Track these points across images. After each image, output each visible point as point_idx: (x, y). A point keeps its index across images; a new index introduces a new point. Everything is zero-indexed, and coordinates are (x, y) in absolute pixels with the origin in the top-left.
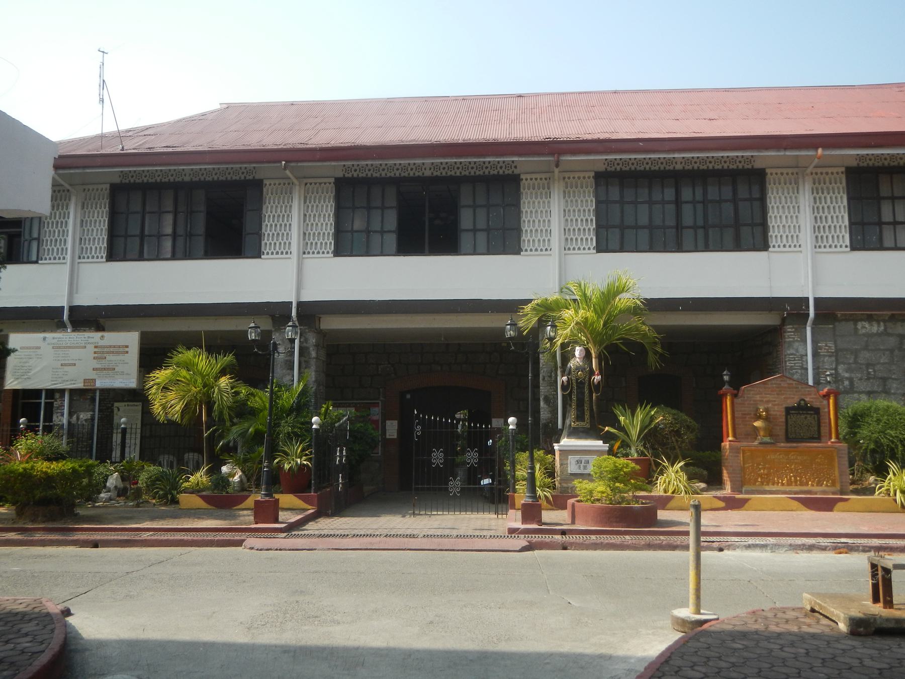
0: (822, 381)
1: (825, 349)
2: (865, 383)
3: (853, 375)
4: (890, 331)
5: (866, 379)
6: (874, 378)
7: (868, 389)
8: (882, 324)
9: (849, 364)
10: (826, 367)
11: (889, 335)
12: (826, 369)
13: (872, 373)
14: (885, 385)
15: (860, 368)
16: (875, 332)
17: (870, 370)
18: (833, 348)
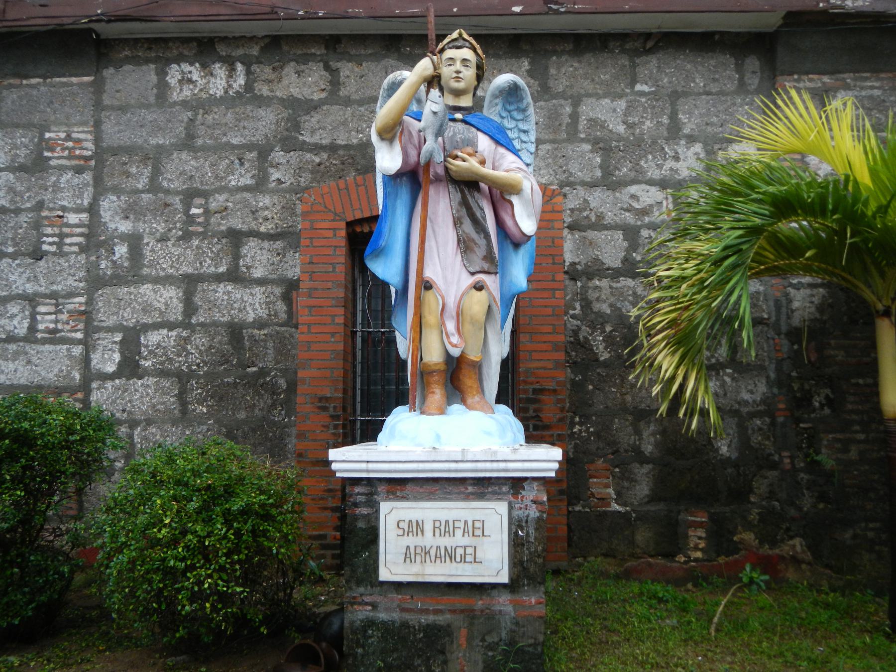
0: (45, 247)
1: (63, 149)
2: (176, 251)
3: (141, 227)
4: (264, 90)
5: (180, 239)
6: (203, 235)
7: (186, 269)
8: (239, 67)
9: (137, 192)
10: (65, 203)
11: (261, 101)
12: (64, 209)
13: (201, 220)
14: (237, 257)
15: (167, 205)
16: (220, 93)
17: (194, 211)
18: (90, 145)
